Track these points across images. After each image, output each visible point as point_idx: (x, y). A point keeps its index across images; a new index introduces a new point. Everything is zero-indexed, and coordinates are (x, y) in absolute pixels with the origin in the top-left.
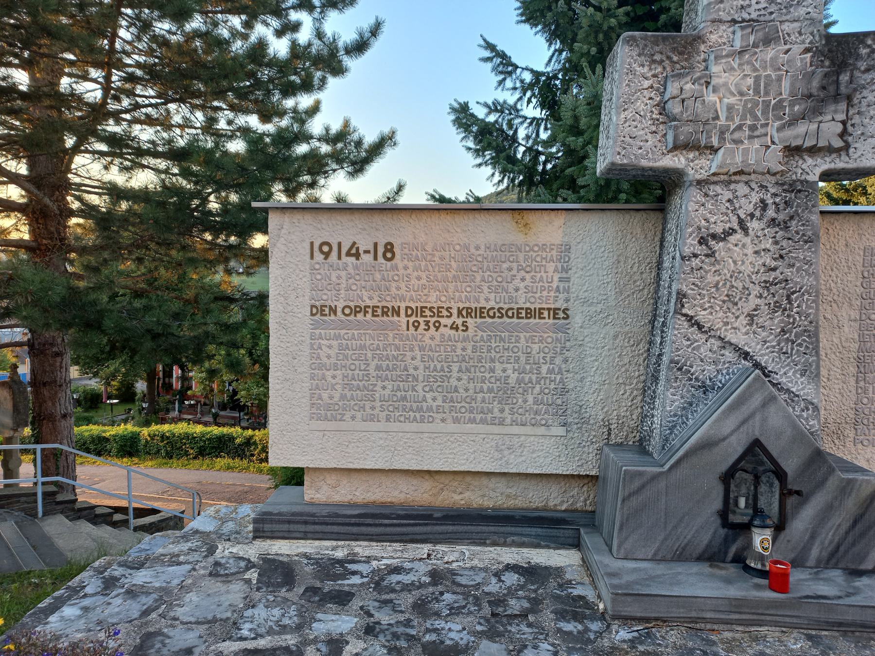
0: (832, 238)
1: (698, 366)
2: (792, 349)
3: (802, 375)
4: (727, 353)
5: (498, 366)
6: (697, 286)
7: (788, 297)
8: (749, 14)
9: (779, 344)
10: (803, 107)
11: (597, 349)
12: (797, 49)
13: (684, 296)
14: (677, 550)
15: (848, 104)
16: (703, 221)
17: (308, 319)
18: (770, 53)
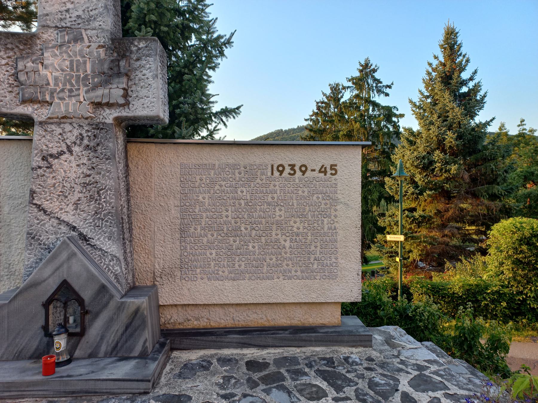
0: (162, 158)
1: (45, 236)
2: (102, 224)
3: (109, 239)
4: (62, 228)
6: (42, 186)
7: (98, 193)
8: (66, 23)
9: (94, 221)
10: (100, 79)
11: (19, 227)
12: (94, 46)
13: (34, 192)
14: (16, 353)
15: (128, 79)
16: (44, 147)
18: (78, 47)
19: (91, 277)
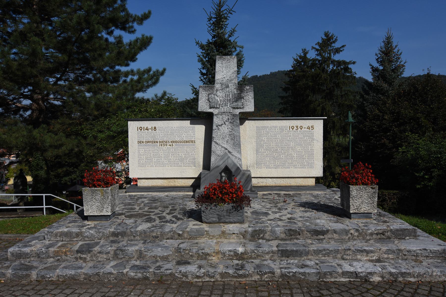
5: (180, 154)
17: (137, 144)
18: (228, 89)
19: (235, 165)
